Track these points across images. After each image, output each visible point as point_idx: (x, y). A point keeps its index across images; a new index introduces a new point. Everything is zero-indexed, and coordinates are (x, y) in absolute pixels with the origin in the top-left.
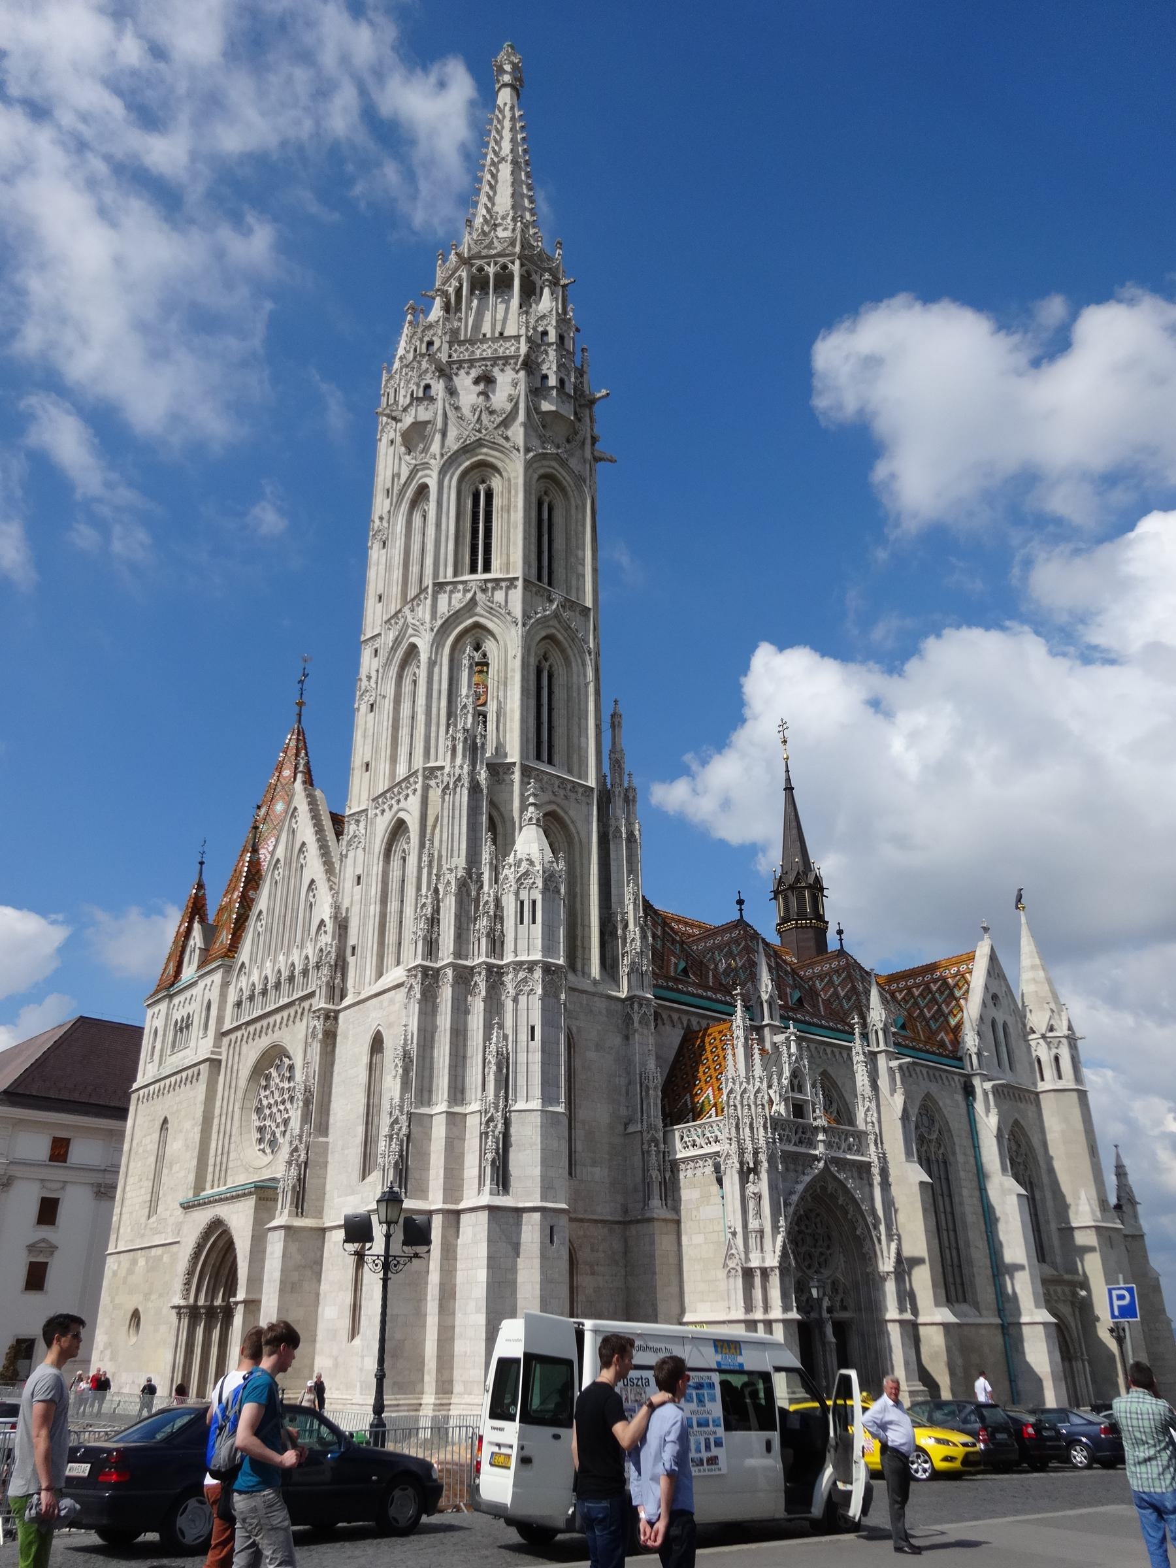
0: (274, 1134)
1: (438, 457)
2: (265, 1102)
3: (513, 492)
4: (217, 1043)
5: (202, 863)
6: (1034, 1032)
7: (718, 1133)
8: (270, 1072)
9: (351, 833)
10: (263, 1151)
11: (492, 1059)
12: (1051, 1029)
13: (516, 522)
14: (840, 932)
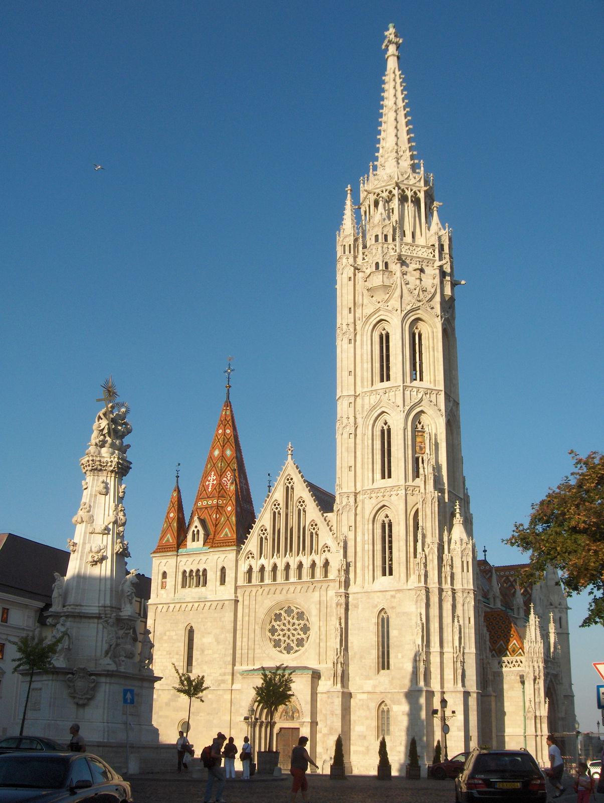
0: (288, 644)
1: (399, 311)
2: (277, 627)
3: (435, 340)
4: (236, 593)
5: (178, 477)
6: (551, 605)
7: (520, 663)
8: (280, 614)
9: (344, 503)
10: (281, 652)
11: (457, 630)
12: (559, 605)
13: (438, 358)
14: (485, 551)
